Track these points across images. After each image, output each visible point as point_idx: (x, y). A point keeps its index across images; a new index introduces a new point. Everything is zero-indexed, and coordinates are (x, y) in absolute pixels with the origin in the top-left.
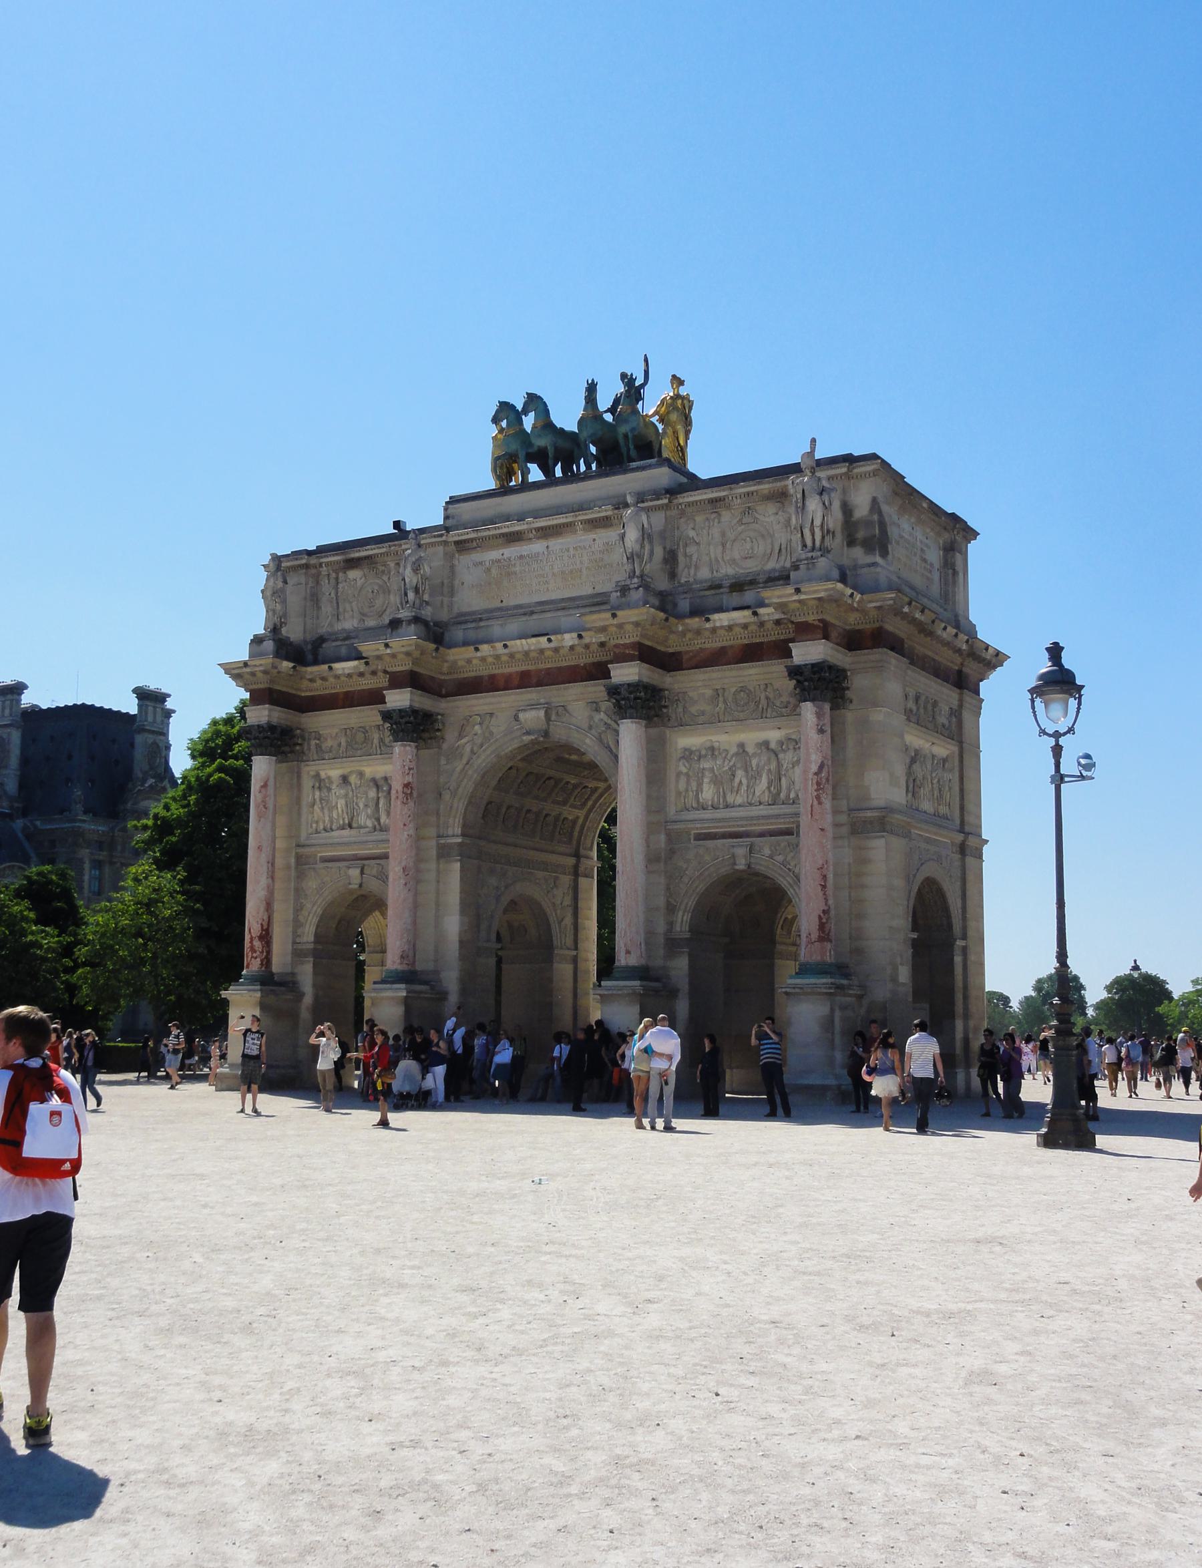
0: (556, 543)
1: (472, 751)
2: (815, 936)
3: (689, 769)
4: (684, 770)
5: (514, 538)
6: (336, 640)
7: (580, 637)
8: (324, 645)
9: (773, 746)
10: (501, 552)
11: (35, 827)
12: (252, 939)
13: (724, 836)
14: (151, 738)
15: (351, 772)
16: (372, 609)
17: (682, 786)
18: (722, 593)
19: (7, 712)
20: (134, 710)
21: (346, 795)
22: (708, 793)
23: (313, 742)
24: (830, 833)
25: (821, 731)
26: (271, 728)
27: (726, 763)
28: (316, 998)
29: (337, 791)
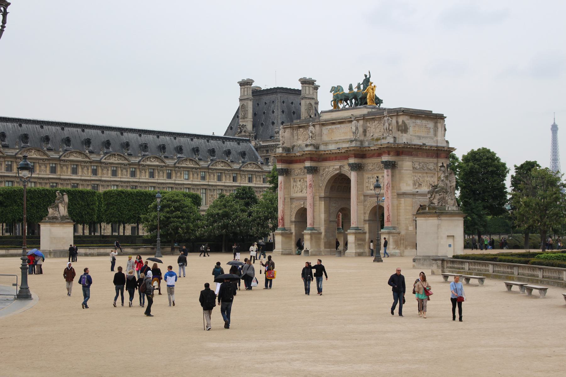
0: (343, 125)
2: (386, 221)
3: (368, 181)
5: (333, 124)
11: (260, 144)
14: (308, 101)
15: (301, 178)
17: (367, 186)
19: (246, 93)
20: (300, 88)
23: (293, 171)
24: (390, 198)
25: (388, 176)
26: (282, 169)
28: (296, 233)
29: (299, 183)
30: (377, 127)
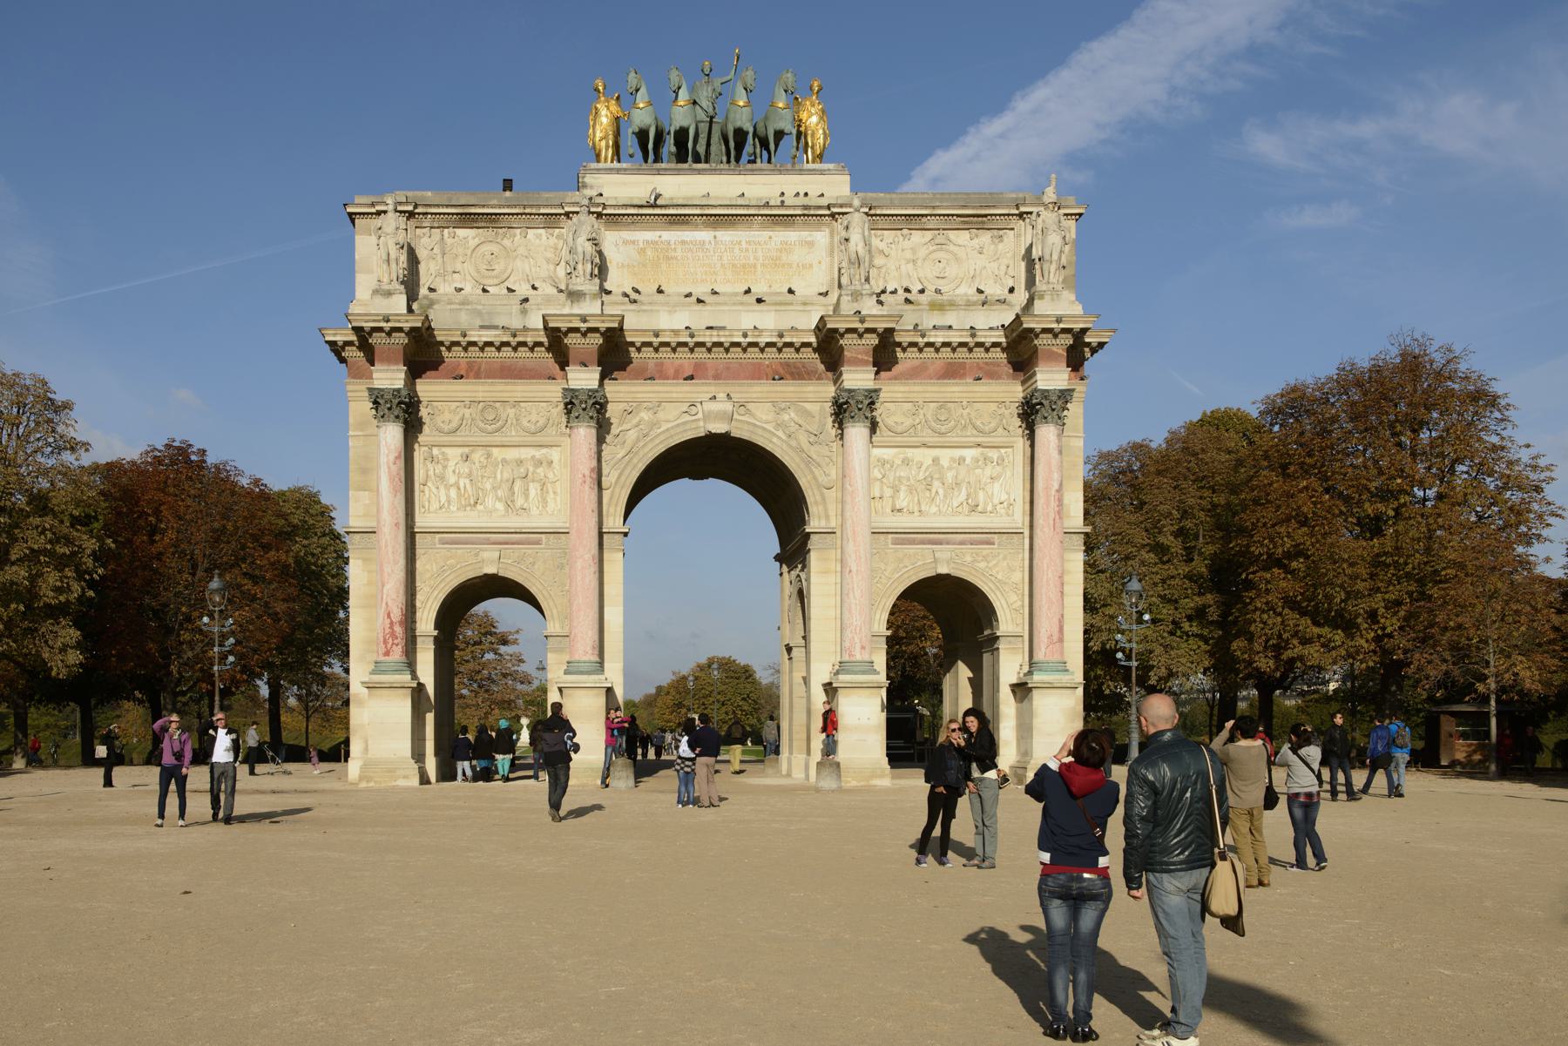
0: (726, 235)
1: (638, 440)
4: (880, 476)
5: (678, 221)
6: (449, 304)
7: (781, 336)
8: (435, 307)
9: (968, 461)
10: (658, 233)
12: (392, 623)
13: (923, 542)
16: (490, 273)
18: (922, 310)
21: (470, 474)
22: (903, 501)
27: (921, 473)
30: (922, 252)
